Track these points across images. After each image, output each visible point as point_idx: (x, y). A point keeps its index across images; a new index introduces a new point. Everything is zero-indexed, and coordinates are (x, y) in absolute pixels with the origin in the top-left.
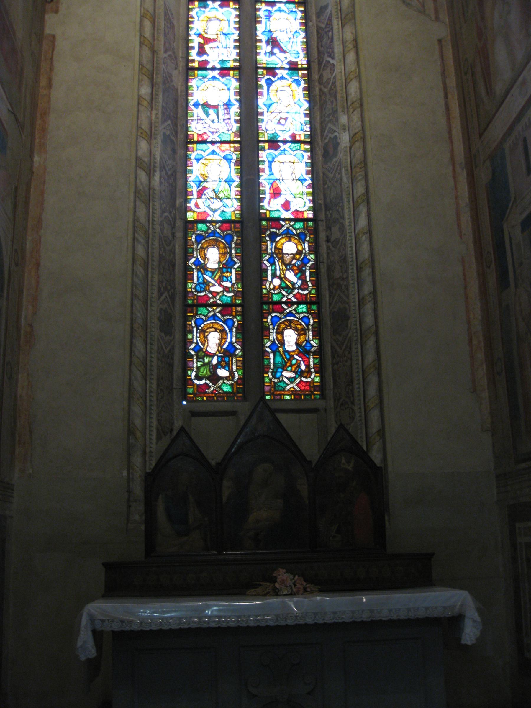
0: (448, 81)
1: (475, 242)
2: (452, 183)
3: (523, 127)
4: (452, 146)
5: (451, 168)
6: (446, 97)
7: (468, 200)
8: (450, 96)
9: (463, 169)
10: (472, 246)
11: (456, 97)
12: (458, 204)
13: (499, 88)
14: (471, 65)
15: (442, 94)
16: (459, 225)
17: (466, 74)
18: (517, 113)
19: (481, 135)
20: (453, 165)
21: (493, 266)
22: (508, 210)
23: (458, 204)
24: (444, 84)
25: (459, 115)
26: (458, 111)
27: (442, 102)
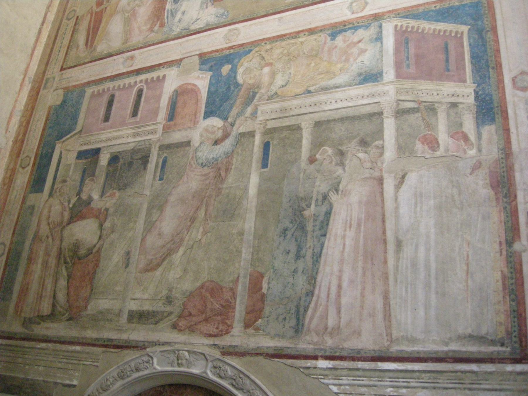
0: (49, 14)
1: (15, 142)
2: (17, 89)
3: (114, 87)
4: (30, 61)
5: (23, 76)
6: (43, 24)
7: (22, 108)
8: (45, 25)
9: (30, 83)
10: (11, 143)
11: (49, 30)
12: (14, 107)
13: (101, 48)
14: (78, 17)
15: (41, 20)
16: (9, 122)
17: (69, 19)
18: (113, 74)
19: (62, 69)
20: (25, 76)
21: (29, 168)
22: (68, 136)
23: (14, 107)
24: (46, 15)
25: (44, 43)
26: (45, 40)
27: (39, 27)
